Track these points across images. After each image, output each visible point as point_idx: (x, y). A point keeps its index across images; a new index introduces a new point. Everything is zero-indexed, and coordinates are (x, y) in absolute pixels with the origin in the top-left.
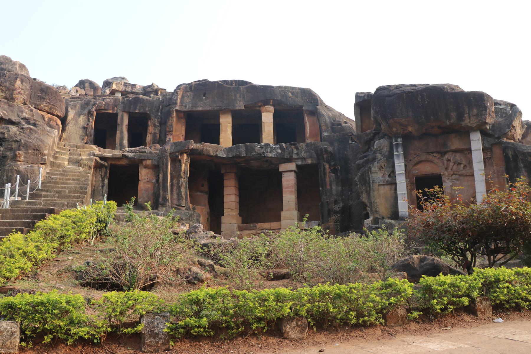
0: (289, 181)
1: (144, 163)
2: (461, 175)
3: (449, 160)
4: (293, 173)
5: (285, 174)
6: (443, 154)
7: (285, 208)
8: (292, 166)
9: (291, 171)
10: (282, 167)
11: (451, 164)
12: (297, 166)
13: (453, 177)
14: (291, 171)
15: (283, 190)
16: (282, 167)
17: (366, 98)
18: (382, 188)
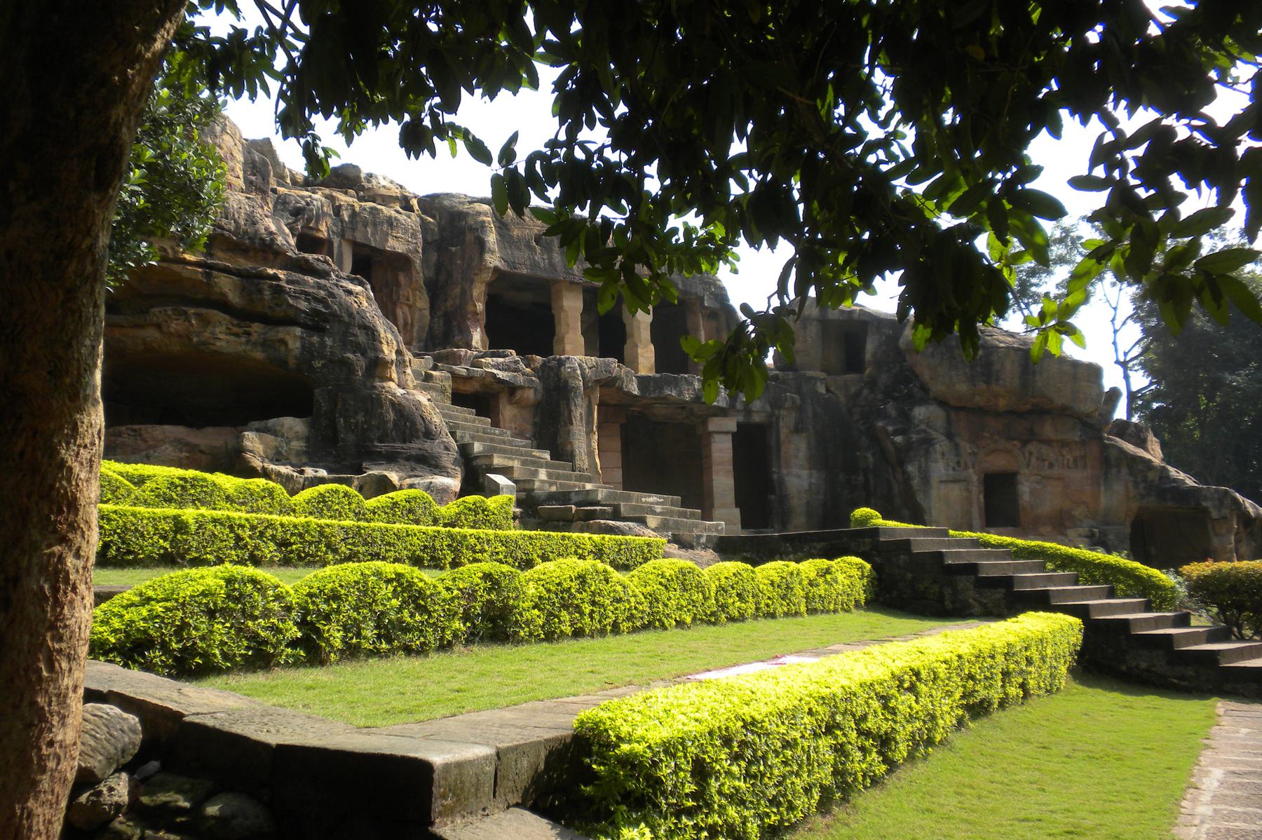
0: (722, 450)
1: (519, 394)
2: (1044, 477)
3: (1031, 453)
4: (730, 437)
5: (716, 437)
6: (1025, 443)
7: (717, 502)
8: (731, 424)
9: (727, 433)
10: (714, 424)
11: (1033, 459)
12: (739, 425)
13: (1033, 478)
14: (727, 433)
15: (715, 468)
16: (714, 424)
17: (856, 316)
18: (943, 486)
